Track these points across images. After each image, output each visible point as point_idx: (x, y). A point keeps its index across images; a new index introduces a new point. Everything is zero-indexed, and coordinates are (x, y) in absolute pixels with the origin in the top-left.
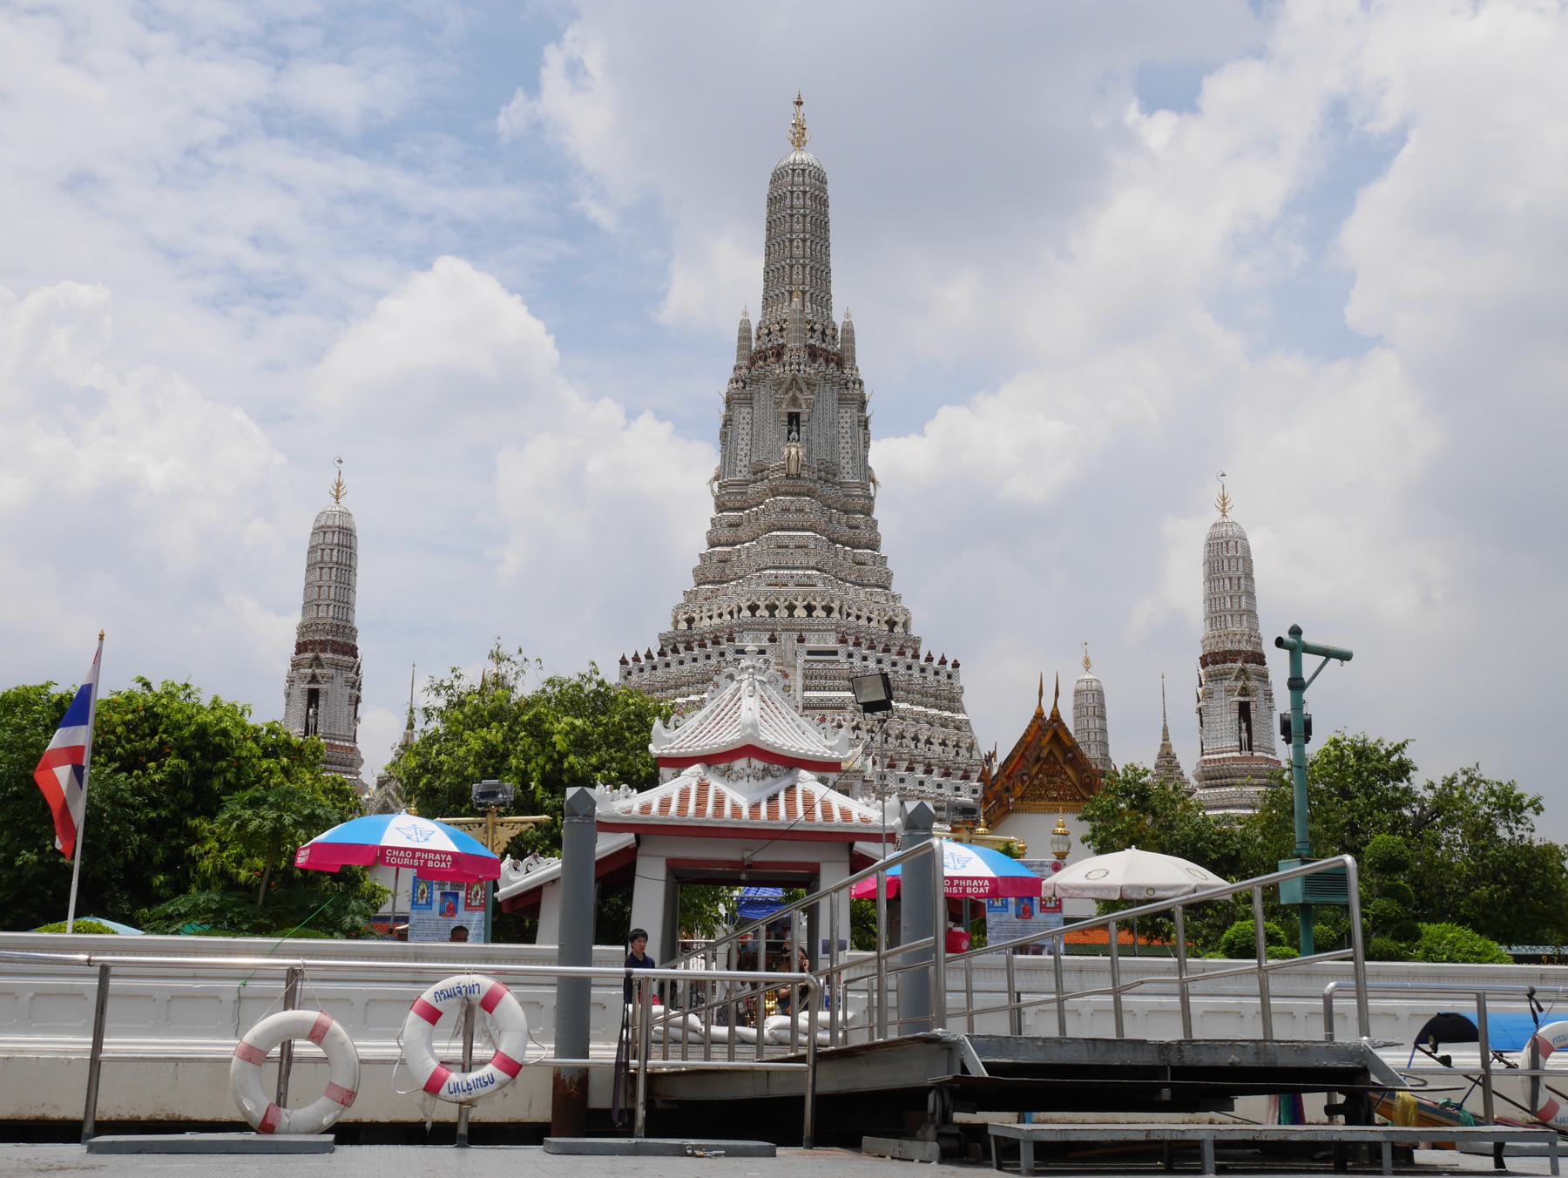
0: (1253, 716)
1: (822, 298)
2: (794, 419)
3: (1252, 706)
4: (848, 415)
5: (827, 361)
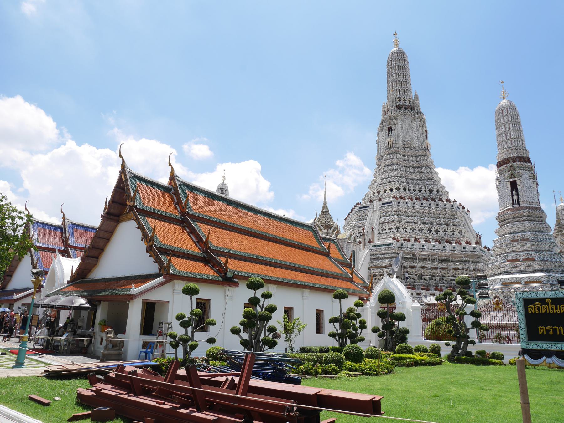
0: (518, 187)
1: (407, 91)
2: (390, 129)
3: (518, 182)
4: (416, 124)
5: (406, 109)
